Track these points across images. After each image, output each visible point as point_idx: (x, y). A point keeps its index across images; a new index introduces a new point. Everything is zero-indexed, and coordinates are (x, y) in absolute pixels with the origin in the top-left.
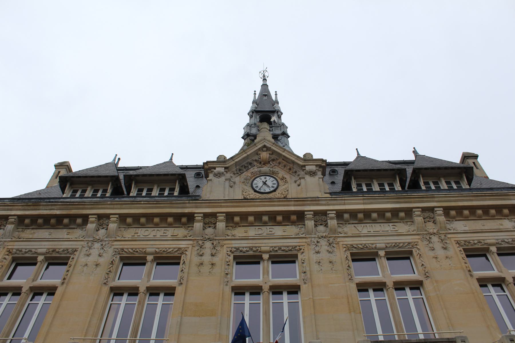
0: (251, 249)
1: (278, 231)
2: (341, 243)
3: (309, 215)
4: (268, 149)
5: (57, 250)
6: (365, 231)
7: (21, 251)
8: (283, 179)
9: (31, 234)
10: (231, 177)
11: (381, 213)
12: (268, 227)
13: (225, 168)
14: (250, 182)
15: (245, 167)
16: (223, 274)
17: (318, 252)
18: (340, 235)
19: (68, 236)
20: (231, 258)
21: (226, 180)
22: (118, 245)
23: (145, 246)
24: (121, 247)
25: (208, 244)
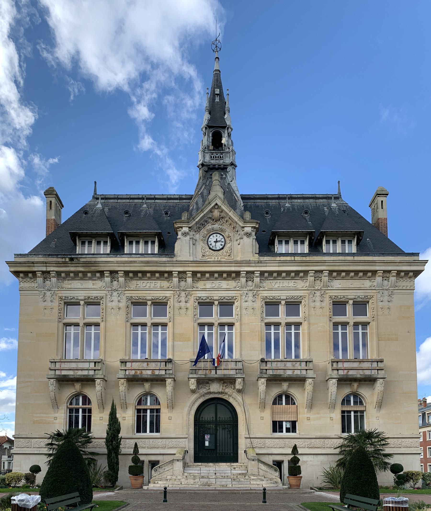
0: (208, 298)
1: (224, 284)
2: (260, 295)
3: (243, 274)
4: (219, 207)
5: (91, 297)
6: (276, 286)
7: (68, 298)
8: (229, 237)
9: (69, 284)
10: (193, 235)
11: (288, 273)
12: (218, 281)
13: (189, 228)
14: (206, 240)
15: (203, 225)
16: (193, 315)
17: (246, 301)
18: (261, 289)
19: (94, 287)
20: (197, 304)
21: (190, 238)
22: (129, 294)
23: (145, 295)
24: (130, 295)
25: (183, 294)
